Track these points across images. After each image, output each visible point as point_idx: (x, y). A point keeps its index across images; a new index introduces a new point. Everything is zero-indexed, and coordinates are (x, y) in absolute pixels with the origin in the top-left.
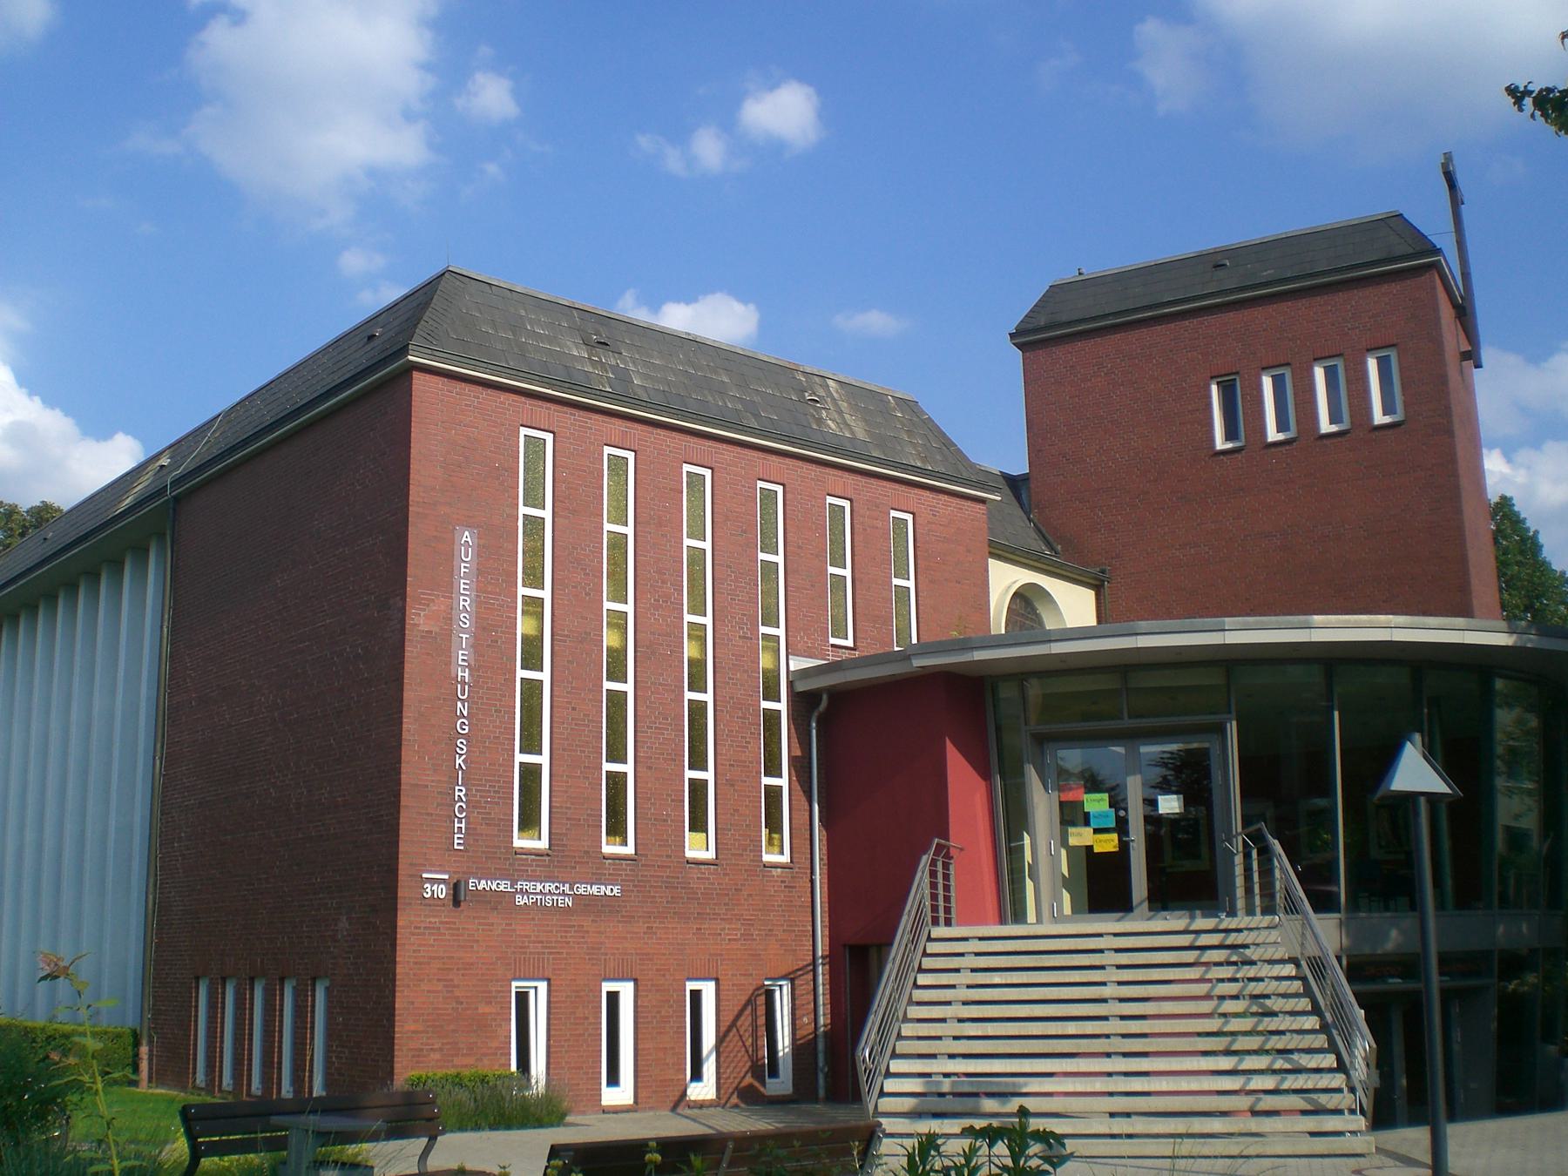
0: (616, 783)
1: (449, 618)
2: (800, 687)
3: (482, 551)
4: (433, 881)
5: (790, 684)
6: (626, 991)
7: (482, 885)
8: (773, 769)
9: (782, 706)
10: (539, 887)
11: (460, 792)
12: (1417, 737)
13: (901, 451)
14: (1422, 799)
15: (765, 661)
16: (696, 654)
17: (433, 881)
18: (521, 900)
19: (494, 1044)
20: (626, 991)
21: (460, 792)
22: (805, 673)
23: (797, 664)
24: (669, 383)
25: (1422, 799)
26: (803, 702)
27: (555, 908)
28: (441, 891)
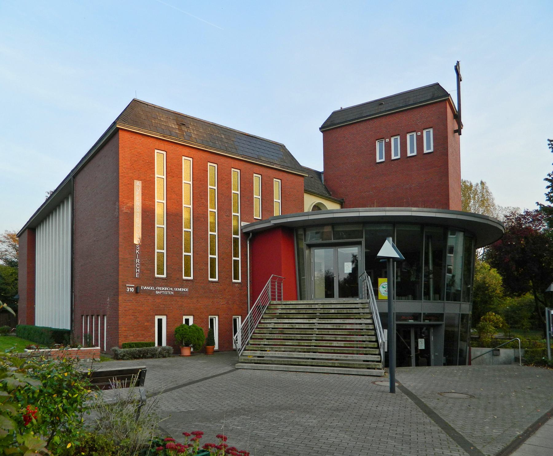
0: (187, 260)
1: (132, 209)
2: (244, 231)
3: (144, 188)
4: (129, 287)
5: (241, 230)
6: (164, 319)
7: (145, 288)
8: (236, 255)
9: (239, 237)
10: (163, 289)
11: (138, 261)
12: (391, 239)
13: (271, 158)
14: (391, 260)
15: (234, 223)
16: (212, 221)
17: (129, 287)
18: (157, 292)
19: (149, 334)
20: (164, 319)
21: (138, 261)
22: (246, 227)
23: (243, 224)
24: (204, 137)
25: (391, 260)
26: (245, 235)
27: (169, 295)
28: (132, 290)
